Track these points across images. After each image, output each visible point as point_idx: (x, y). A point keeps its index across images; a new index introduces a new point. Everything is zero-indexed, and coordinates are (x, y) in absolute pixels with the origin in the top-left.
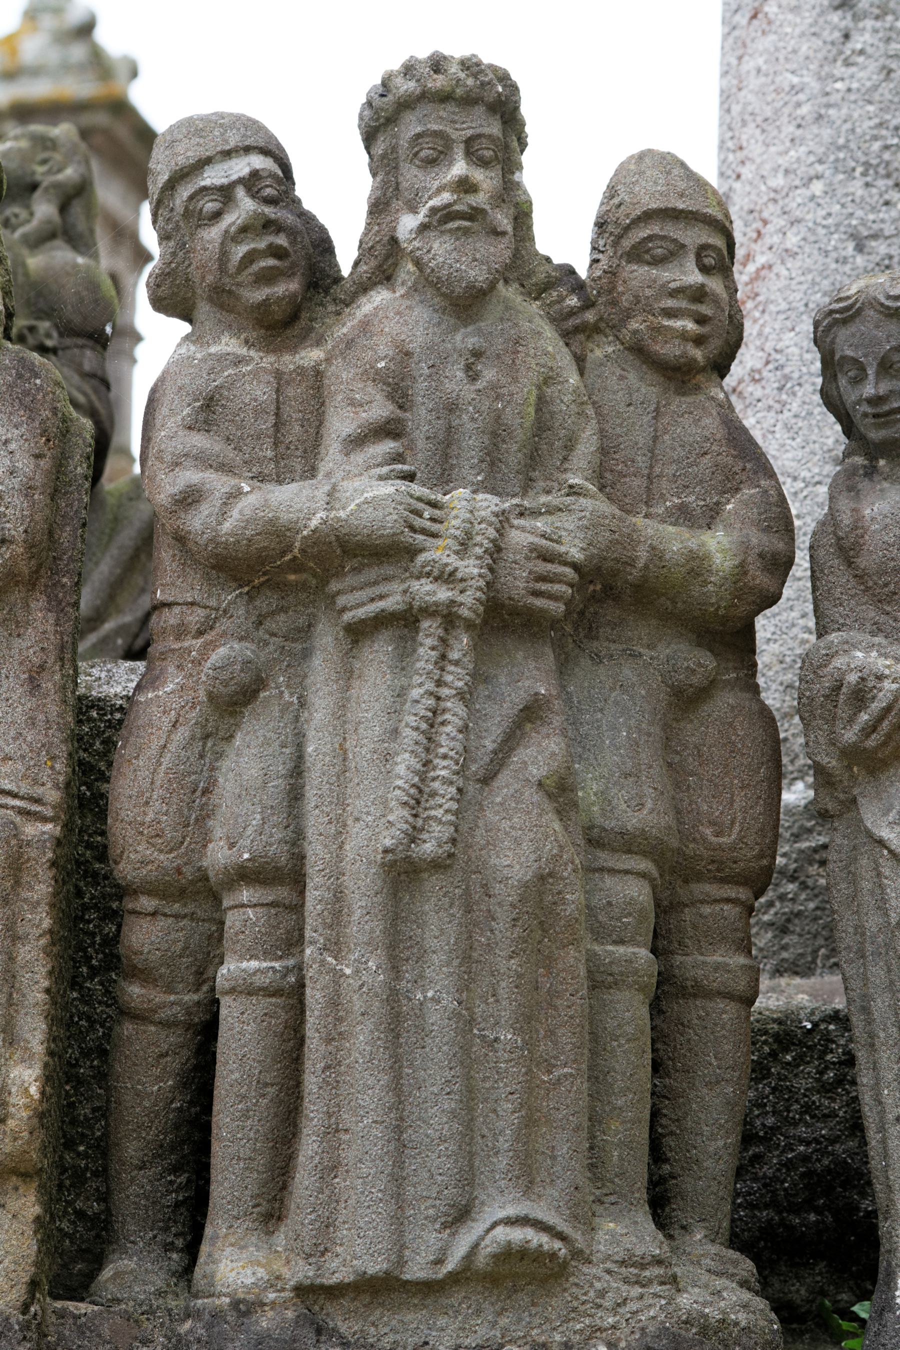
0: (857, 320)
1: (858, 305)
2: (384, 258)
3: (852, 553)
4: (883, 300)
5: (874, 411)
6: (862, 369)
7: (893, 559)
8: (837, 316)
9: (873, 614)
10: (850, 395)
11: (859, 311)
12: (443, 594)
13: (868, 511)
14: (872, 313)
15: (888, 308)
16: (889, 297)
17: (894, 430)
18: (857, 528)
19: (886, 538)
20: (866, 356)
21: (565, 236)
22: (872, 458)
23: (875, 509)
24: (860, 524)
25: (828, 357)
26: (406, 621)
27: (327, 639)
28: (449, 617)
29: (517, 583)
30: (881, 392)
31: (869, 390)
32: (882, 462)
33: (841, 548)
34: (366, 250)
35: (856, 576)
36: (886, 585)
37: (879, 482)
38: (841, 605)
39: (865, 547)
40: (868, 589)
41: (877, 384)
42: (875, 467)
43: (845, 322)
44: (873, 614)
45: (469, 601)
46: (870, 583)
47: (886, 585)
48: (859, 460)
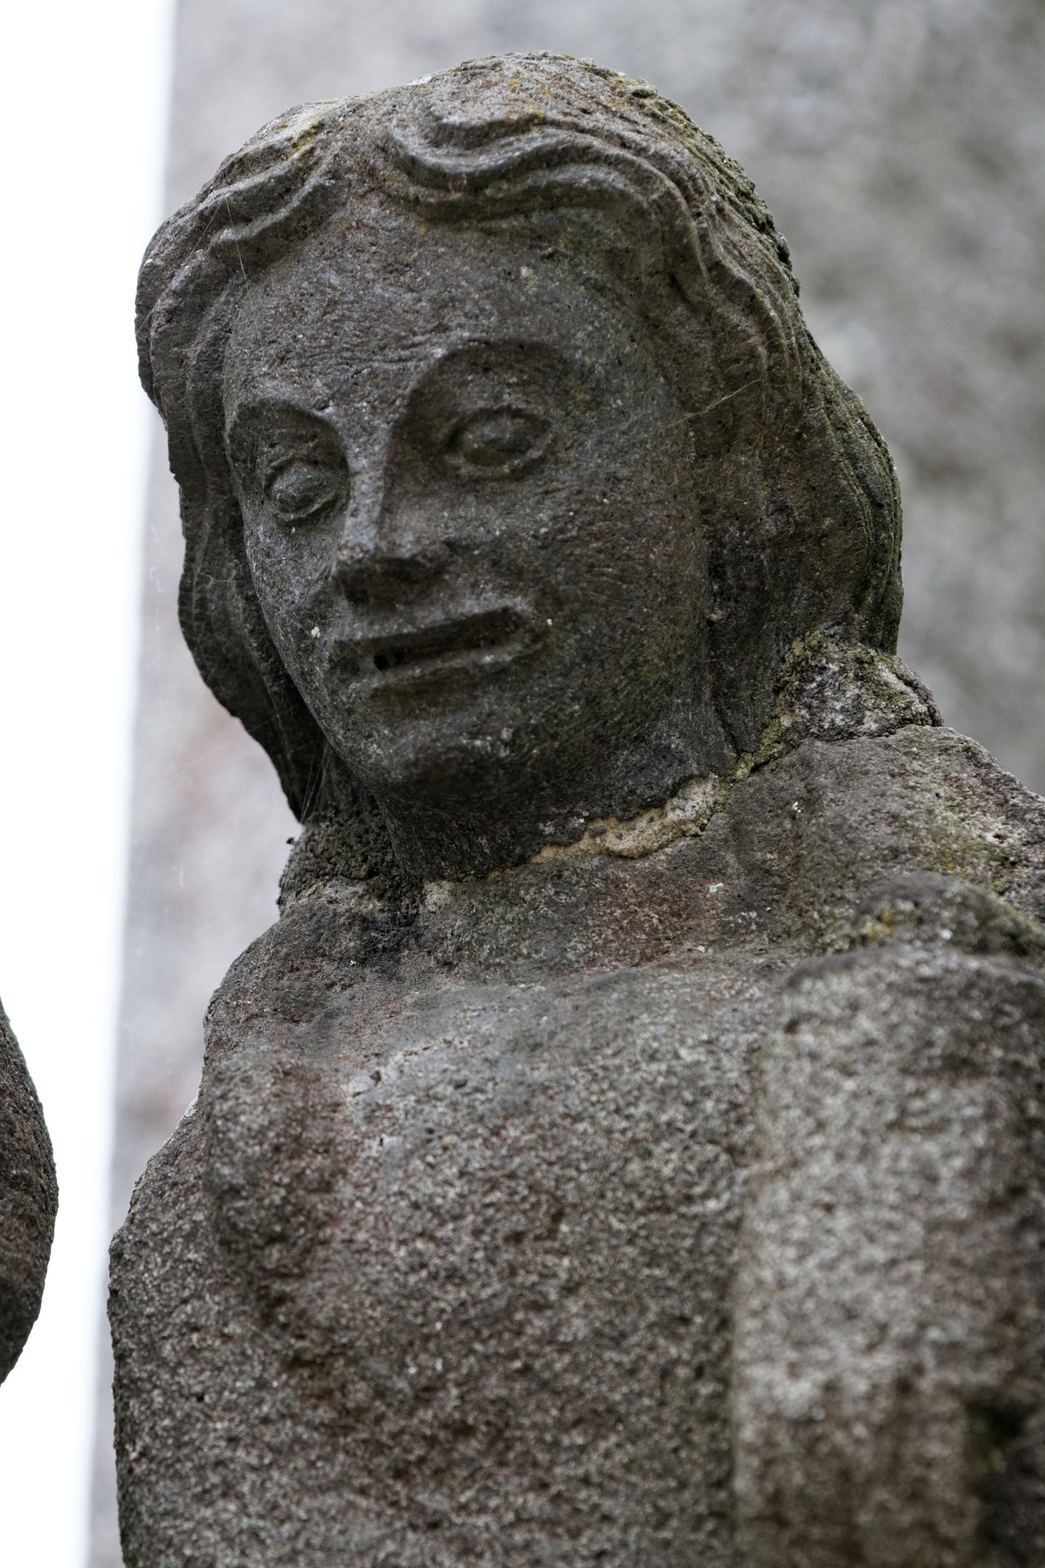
0: (311, 248)
1: (314, 180)
3: (275, 1255)
4: (415, 146)
5: (376, 631)
6: (334, 461)
7: (453, 1276)
8: (227, 234)
9: (373, 1531)
10: (289, 574)
11: (318, 211)
13: (360, 1082)
14: (372, 210)
15: (438, 178)
16: (442, 134)
17: (468, 719)
18: (298, 1148)
19: (427, 1187)
20: (342, 396)
22: (398, 887)
23: (389, 1073)
24: (315, 1134)
25: (198, 433)
30: (407, 546)
31: (356, 534)
32: (437, 894)
33: (230, 1238)
35: (294, 1363)
36: (426, 1393)
37: (423, 978)
38: (228, 1490)
39: (338, 1233)
40: (350, 1418)
41: (387, 509)
42: (410, 921)
43: (260, 258)
44: (373, 1531)
46: (360, 1393)
47: (426, 1393)
48: (343, 896)
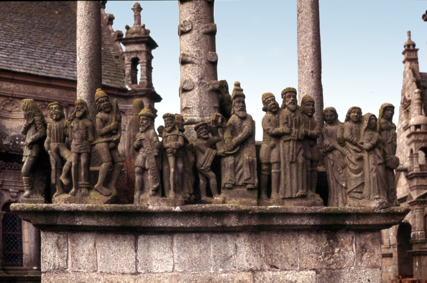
2: (284, 106)
12: (294, 138)
21: (299, 103)
26: (289, 141)
27: (282, 141)
28: (294, 140)
29: (300, 137)
34: (282, 105)
45: (296, 139)
